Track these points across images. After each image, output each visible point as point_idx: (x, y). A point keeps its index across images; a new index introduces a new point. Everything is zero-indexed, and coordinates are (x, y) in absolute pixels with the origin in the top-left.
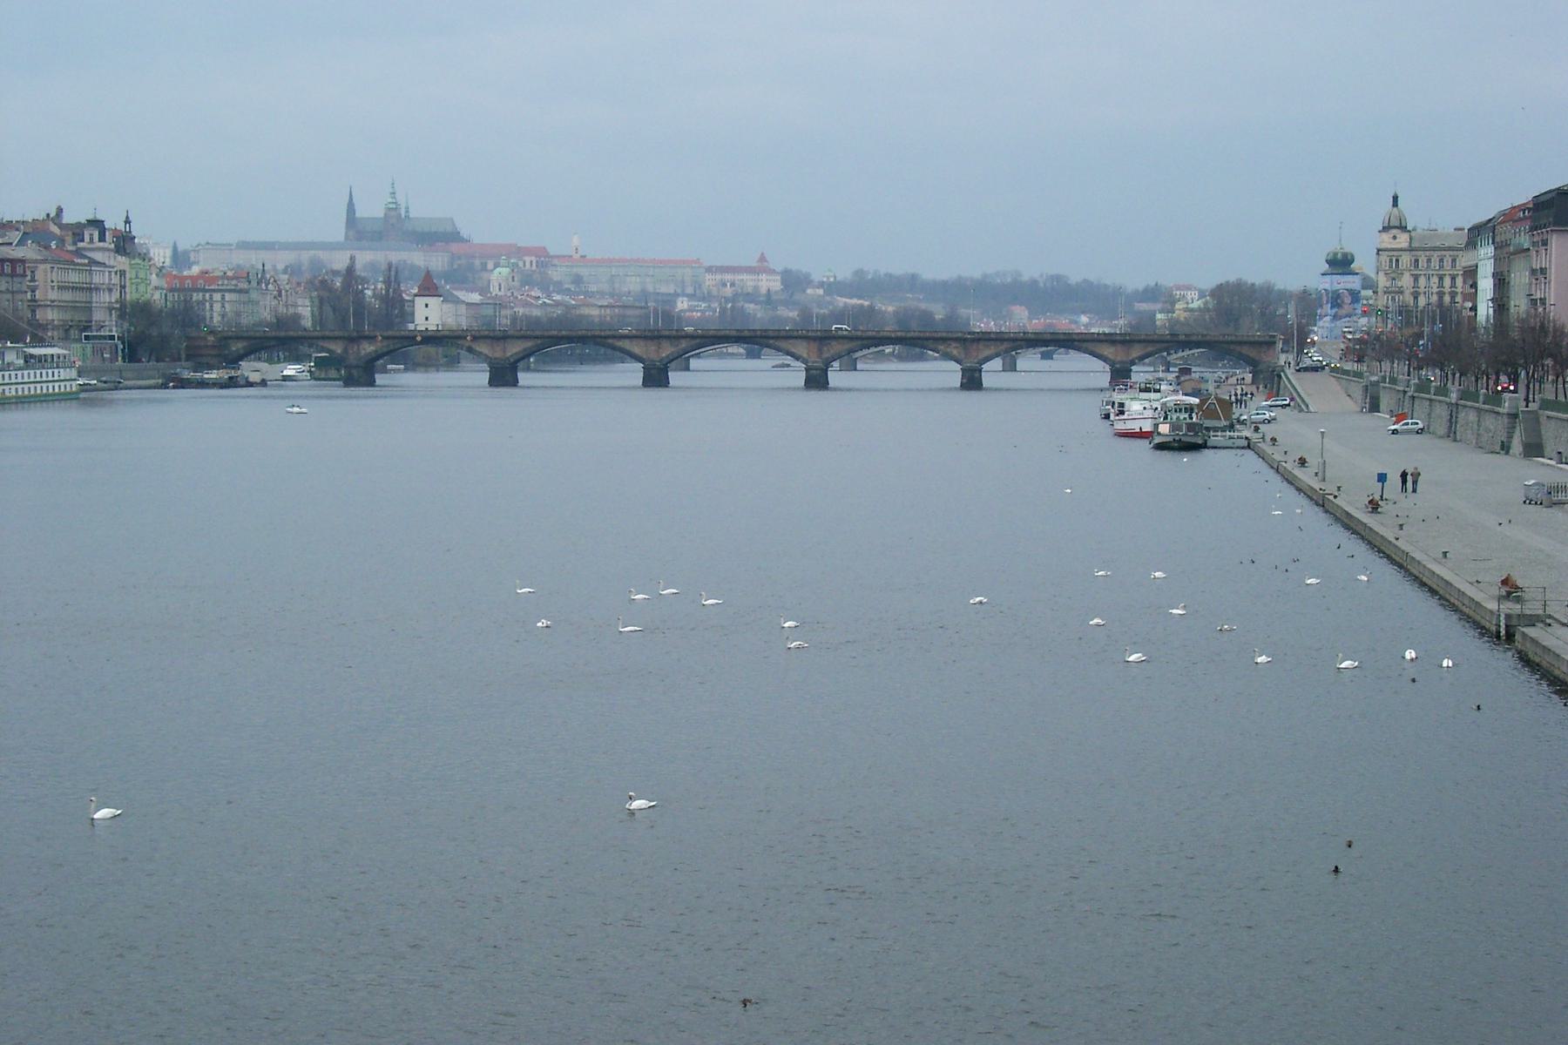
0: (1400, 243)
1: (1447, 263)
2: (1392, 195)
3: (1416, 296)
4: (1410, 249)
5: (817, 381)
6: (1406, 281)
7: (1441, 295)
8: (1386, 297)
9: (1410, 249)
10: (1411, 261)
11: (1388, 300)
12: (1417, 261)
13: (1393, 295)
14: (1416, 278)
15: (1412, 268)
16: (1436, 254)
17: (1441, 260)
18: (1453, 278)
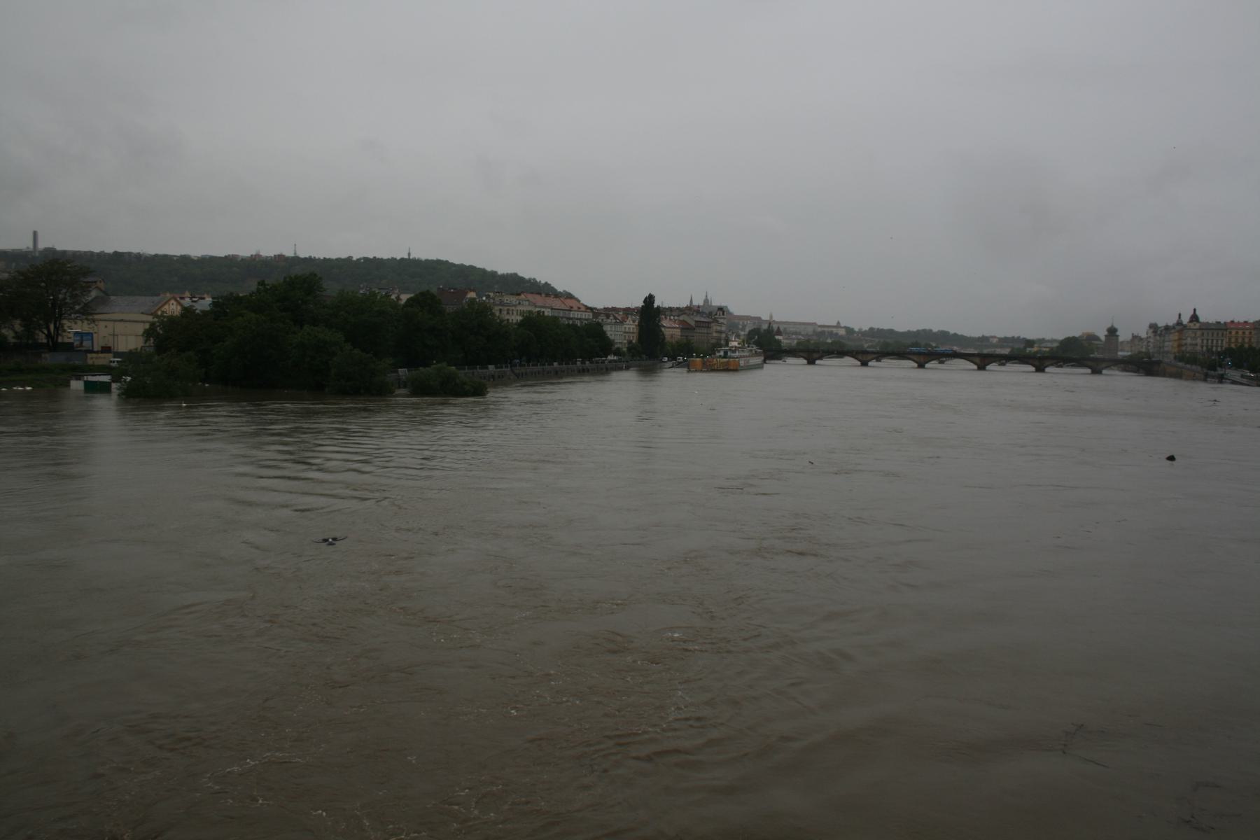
1: (1215, 335)
3: (1202, 347)
4: (1200, 329)
5: (921, 366)
6: (1199, 341)
9: (1200, 329)
14: (1203, 340)
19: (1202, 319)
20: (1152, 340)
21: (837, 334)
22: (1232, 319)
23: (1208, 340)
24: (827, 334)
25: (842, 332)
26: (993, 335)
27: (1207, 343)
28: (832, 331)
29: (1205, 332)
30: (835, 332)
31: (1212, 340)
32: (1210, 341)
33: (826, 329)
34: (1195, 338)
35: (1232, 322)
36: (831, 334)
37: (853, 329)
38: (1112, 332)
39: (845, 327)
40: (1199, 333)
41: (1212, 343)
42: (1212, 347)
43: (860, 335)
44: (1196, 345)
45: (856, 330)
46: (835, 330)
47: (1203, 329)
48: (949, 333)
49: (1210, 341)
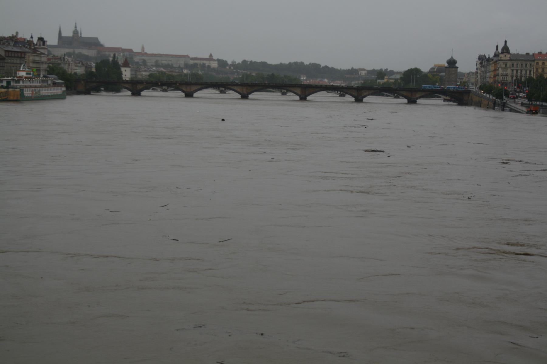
0: (507, 58)
2: (505, 40)
3: (512, 77)
6: (509, 72)
7: (517, 76)
8: (502, 77)
9: (510, 60)
10: (511, 65)
11: (503, 78)
12: (513, 65)
13: (504, 76)
14: (513, 71)
15: (511, 67)
16: (520, 62)
17: (517, 65)
18: (517, 71)
19: (512, 50)
20: (479, 72)
21: (209, 66)
22: (540, 51)
23: (517, 71)
24: (199, 66)
25: (214, 65)
26: (362, 67)
27: (517, 73)
28: (204, 64)
29: (515, 63)
30: (207, 64)
31: (526, 71)
32: (519, 71)
33: (198, 62)
34: (505, 69)
35: (540, 53)
36: (203, 66)
37: (226, 61)
38: (452, 63)
39: (218, 60)
40: (509, 64)
41: (521, 73)
42: (521, 77)
43: (232, 68)
44: (507, 75)
45: (229, 62)
46: (207, 63)
47: (514, 60)
48: (319, 65)
49: (519, 71)
